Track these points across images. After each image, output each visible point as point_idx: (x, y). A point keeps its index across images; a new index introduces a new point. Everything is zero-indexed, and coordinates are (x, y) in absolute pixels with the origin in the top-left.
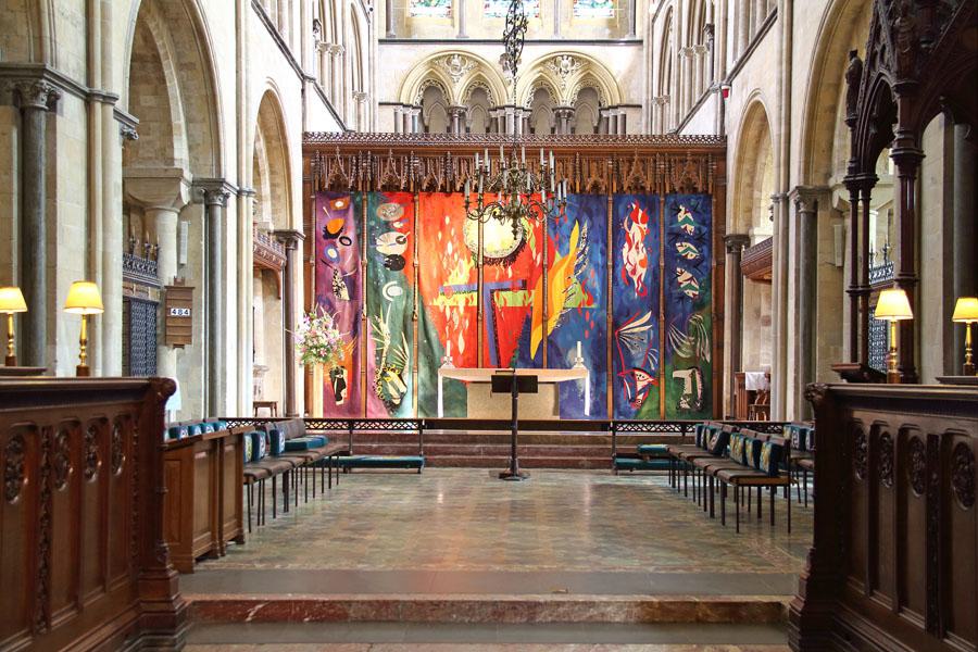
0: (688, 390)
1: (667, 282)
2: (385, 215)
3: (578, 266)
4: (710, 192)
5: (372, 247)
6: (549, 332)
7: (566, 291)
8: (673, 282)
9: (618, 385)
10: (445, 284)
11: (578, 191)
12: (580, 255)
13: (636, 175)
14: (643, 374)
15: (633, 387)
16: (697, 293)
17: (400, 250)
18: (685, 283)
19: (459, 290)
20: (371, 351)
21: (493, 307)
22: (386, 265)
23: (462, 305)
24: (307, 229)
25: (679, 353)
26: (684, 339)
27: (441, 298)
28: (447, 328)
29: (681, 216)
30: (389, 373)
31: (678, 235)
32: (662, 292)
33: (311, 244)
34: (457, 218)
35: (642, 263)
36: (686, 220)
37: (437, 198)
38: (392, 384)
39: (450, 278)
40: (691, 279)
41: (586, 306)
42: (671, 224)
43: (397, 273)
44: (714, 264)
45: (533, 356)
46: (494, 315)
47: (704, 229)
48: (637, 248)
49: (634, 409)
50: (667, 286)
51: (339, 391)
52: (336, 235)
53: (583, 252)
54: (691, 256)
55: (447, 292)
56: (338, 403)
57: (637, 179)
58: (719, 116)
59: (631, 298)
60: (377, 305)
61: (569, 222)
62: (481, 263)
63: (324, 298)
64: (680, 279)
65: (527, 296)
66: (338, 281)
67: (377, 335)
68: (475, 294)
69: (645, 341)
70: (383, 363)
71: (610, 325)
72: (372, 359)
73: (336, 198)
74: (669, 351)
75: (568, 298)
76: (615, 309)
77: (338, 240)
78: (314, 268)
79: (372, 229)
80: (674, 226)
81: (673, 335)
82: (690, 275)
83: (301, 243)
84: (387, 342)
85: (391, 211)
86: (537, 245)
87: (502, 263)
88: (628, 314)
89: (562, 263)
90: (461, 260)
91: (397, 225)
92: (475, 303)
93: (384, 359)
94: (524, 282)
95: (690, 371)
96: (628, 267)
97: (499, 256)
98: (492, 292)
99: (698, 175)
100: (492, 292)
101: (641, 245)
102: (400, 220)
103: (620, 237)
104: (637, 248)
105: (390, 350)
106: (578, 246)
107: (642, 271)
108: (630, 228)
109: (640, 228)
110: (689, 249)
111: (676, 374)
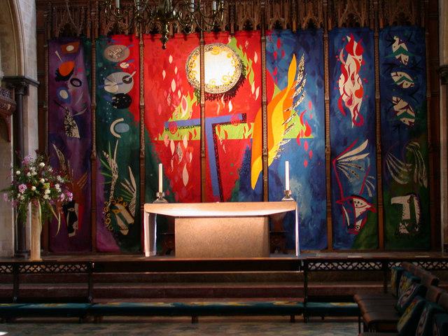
0: (406, 215)
1: (383, 111)
2: (112, 57)
4: (423, 26)
5: (99, 87)
6: (270, 161)
7: (285, 123)
8: (390, 111)
10: (170, 120)
11: (294, 29)
14: (361, 201)
15: (352, 213)
17: (127, 89)
19: (183, 124)
20: (101, 184)
23: (185, 140)
25: (398, 181)
28: (172, 161)
30: (118, 205)
31: (394, 65)
32: (378, 125)
33: (45, 90)
34: (180, 57)
35: (358, 94)
36: (400, 50)
38: (120, 215)
39: (174, 114)
40: (407, 107)
41: (304, 137)
42: (386, 54)
43: (126, 111)
44: (429, 95)
46: (216, 148)
47: (419, 59)
48: (353, 79)
49: (353, 236)
50: (383, 115)
51: (72, 221)
53: (300, 84)
54: (406, 85)
55: (173, 127)
56: (71, 235)
59: (348, 127)
60: (105, 140)
61: (286, 57)
64: (396, 108)
65: (247, 128)
66: (69, 120)
68: (198, 129)
73: (68, 43)
75: (287, 130)
80: (389, 56)
81: (391, 163)
82: (405, 104)
83: (33, 91)
85: (116, 52)
86: (255, 79)
87: (222, 98)
88: (345, 143)
89: (281, 96)
90: (184, 97)
91: (124, 66)
92: (198, 137)
93: (112, 192)
94: (244, 116)
95: (408, 197)
96: (345, 98)
98: (214, 126)
99: (411, 8)
100: (214, 126)
101: (356, 77)
102: (126, 61)
103: (336, 69)
104: (353, 79)
105: (118, 184)
106: (296, 79)
107: (358, 101)
108: (345, 60)
109: (355, 60)
110: (404, 78)
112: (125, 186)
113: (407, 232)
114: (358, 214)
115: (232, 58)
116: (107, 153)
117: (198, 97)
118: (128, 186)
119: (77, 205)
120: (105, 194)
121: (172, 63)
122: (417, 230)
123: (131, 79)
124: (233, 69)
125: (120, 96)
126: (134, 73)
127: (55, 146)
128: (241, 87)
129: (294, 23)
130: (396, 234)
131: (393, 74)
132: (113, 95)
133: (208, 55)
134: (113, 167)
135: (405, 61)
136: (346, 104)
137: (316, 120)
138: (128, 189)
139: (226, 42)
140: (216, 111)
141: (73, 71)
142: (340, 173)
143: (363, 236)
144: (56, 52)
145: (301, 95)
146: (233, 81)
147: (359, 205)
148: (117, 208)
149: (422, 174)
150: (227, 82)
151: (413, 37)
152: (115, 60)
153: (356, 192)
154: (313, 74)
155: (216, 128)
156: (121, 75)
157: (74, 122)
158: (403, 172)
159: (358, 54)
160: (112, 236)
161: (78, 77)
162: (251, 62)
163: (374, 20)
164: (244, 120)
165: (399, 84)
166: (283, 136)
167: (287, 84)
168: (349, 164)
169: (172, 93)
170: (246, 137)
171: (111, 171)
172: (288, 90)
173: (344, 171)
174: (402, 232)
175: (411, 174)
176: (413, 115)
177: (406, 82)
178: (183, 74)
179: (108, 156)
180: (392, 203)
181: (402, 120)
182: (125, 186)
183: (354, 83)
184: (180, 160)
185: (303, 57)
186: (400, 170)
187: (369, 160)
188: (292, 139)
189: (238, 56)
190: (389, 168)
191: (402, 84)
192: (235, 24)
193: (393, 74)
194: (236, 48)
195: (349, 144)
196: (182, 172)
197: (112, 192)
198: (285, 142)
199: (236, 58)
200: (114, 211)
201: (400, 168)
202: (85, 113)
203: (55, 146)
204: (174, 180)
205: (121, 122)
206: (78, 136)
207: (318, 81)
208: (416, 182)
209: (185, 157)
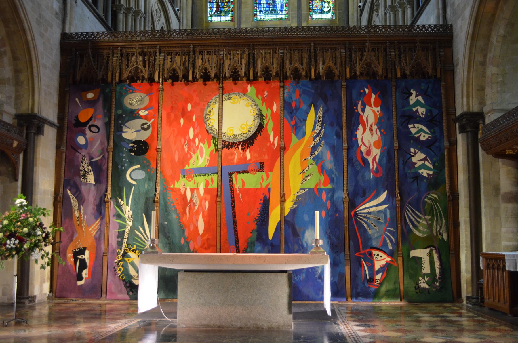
0: (426, 269)
1: (401, 162)
2: (131, 104)
3: (314, 148)
6: (287, 212)
7: (302, 172)
8: (408, 162)
9: (356, 264)
10: (187, 167)
12: (316, 137)
13: (368, 61)
14: (381, 254)
15: (371, 267)
16: (431, 173)
17: (144, 136)
18: (419, 164)
19: (200, 172)
20: (113, 233)
21: (232, 189)
22: (131, 151)
24: (61, 117)
25: (417, 233)
26: (420, 218)
27: (182, 181)
28: (188, 209)
29: (413, 99)
30: (130, 254)
31: (413, 118)
34: (198, 104)
36: (418, 103)
37: (179, 86)
38: (133, 264)
39: (191, 161)
40: (425, 159)
41: (322, 187)
42: (403, 107)
43: (140, 157)
45: (270, 237)
46: (232, 197)
47: (435, 112)
48: (371, 130)
50: (402, 167)
52: (85, 124)
53: (318, 134)
54: (424, 137)
55: (190, 174)
56: (79, 283)
57: (369, 64)
58: (441, 11)
59: (367, 178)
61: (304, 107)
62: (220, 147)
63: (72, 182)
64: (414, 159)
65: (265, 177)
66: (85, 166)
67: (119, 216)
68: (215, 177)
70: (124, 245)
71: (346, 205)
72: (113, 241)
73: (88, 90)
74: (405, 231)
75: (304, 180)
76: (351, 189)
77: (87, 127)
78: (64, 154)
79: (119, 117)
81: (409, 215)
82: (423, 156)
84: (130, 224)
86: (273, 129)
87: (240, 147)
90: (201, 144)
92: (215, 185)
93: (125, 240)
95: (428, 250)
96: (363, 149)
97: (238, 139)
98: (231, 174)
102: (145, 109)
104: (371, 130)
106: (314, 129)
107: (376, 152)
108: (363, 110)
109: (373, 111)
110: (421, 130)
111: (415, 253)
112: (138, 233)
113: (427, 287)
115: (250, 107)
116: (122, 200)
117: (215, 145)
118: (141, 233)
119: (87, 252)
120: (118, 241)
122: (438, 284)
123: (149, 126)
124: (252, 118)
125: (137, 142)
126: (153, 120)
127: (69, 192)
128: (259, 135)
129: (313, 70)
130: (416, 289)
132: (130, 141)
133: (226, 104)
134: (127, 214)
135: (422, 114)
136: (365, 155)
137: (334, 171)
138: (142, 237)
139: (245, 91)
140: (233, 159)
141: (92, 117)
142: (360, 226)
144: (77, 99)
145: (319, 145)
146: (251, 130)
148: (129, 257)
149: (441, 227)
150: (246, 131)
151: (429, 90)
152: (135, 107)
153: (375, 244)
154: (331, 125)
155: (233, 176)
157: (90, 168)
158: (423, 225)
159: (376, 106)
160: (123, 286)
161: (96, 123)
162: (270, 111)
163: (391, 70)
165: (416, 136)
166: (299, 186)
167: (304, 134)
168: (368, 216)
169: (189, 141)
170: (264, 186)
172: (305, 142)
173: (362, 222)
174: (422, 287)
175: (430, 226)
176: (431, 167)
177: (423, 134)
178: (202, 120)
179: (122, 202)
180: (411, 256)
181: (420, 171)
182: (138, 233)
184: (196, 208)
185: (321, 108)
186: (419, 222)
187: (388, 211)
188: (310, 189)
189: (257, 105)
190: (408, 220)
191: (419, 136)
192: (254, 71)
194: (255, 97)
195: (367, 195)
196: (197, 220)
197: (125, 240)
198: (302, 192)
200: (126, 259)
201: (418, 219)
202: (101, 159)
203: (69, 192)
204: (189, 229)
205: (138, 169)
206: (93, 182)
207: (336, 131)
208: (435, 234)
209: (200, 205)
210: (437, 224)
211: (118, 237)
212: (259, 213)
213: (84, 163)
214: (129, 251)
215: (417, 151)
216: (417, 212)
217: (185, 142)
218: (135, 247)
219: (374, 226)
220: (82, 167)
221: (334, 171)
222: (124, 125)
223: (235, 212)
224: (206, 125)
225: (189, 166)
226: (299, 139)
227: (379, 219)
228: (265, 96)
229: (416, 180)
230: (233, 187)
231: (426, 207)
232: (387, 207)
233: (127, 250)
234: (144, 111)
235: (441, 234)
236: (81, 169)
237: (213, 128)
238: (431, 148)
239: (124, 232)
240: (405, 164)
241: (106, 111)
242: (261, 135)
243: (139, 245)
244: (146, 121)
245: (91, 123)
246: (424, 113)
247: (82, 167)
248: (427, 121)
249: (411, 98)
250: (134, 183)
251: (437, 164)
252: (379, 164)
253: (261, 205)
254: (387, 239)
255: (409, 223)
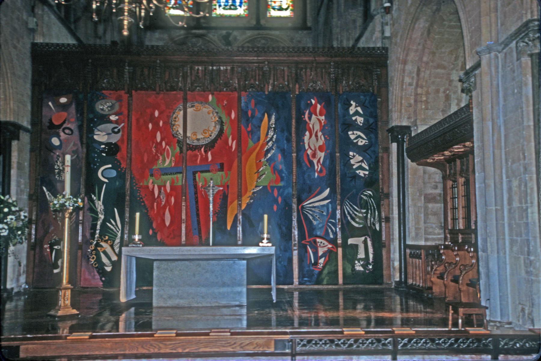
8: (347, 164)
14: (324, 241)
15: (316, 253)
17: (115, 139)
19: (166, 172)
23: (168, 185)
28: (155, 203)
29: (352, 110)
30: (103, 244)
31: (353, 126)
36: (357, 113)
38: (105, 253)
40: (362, 161)
41: (274, 185)
42: (344, 116)
46: (196, 193)
47: (371, 121)
49: (316, 271)
53: (271, 139)
54: (361, 143)
59: (312, 177)
65: (224, 177)
69: (325, 213)
70: (97, 236)
77: (61, 130)
84: (102, 217)
87: (203, 149)
90: (168, 147)
91: (113, 118)
93: (98, 232)
94: (222, 165)
95: (363, 238)
96: (309, 152)
97: (201, 143)
98: (194, 173)
101: (320, 134)
102: (116, 114)
104: (316, 136)
105: (103, 225)
107: (321, 155)
108: (310, 118)
109: (319, 120)
110: (359, 137)
114: (320, 253)
116: (95, 196)
121: (158, 117)
126: (123, 124)
127: (44, 188)
128: (219, 139)
131: (350, 133)
135: (361, 123)
137: (285, 170)
143: (325, 272)
144: (50, 104)
145: (271, 148)
147: (322, 245)
148: (101, 246)
149: (374, 219)
151: (367, 102)
152: (106, 112)
154: (282, 131)
155: (197, 175)
156: (111, 126)
158: (359, 217)
159: (321, 114)
161: (69, 126)
164: (222, 169)
165: (355, 141)
168: (313, 209)
169: (157, 144)
171: (97, 212)
173: (308, 215)
176: (367, 168)
177: (361, 140)
178: (169, 125)
181: (357, 172)
183: (317, 140)
184: (163, 203)
186: (356, 215)
187: (330, 205)
189: (217, 113)
190: (346, 213)
191: (357, 142)
193: (350, 133)
196: (164, 214)
197: (98, 232)
199: (215, 114)
200: (99, 249)
208: (369, 225)
210: (371, 217)
211: (91, 229)
212: (219, 207)
213: (59, 162)
214: (102, 241)
215: (355, 154)
216: (354, 206)
217: (153, 145)
218: (107, 237)
219: (319, 218)
220: (56, 166)
221: (285, 170)
222: (96, 128)
223: (198, 207)
224: (171, 130)
225: (156, 166)
226: (254, 143)
227: (323, 212)
228: (224, 104)
229: (354, 180)
230: (196, 185)
231: (362, 202)
232: (329, 202)
233: (99, 240)
234: (114, 116)
235: (374, 225)
236: (56, 168)
237: (178, 133)
238: (367, 152)
239: (96, 224)
240: (345, 165)
241: (79, 115)
242: (221, 139)
243: (111, 235)
244: (116, 125)
245: (64, 126)
246: (362, 122)
247: (56, 166)
248: (365, 129)
249: (351, 108)
250: (106, 181)
251: (372, 166)
252: (323, 165)
253: (221, 200)
254: (329, 229)
255: (348, 215)
